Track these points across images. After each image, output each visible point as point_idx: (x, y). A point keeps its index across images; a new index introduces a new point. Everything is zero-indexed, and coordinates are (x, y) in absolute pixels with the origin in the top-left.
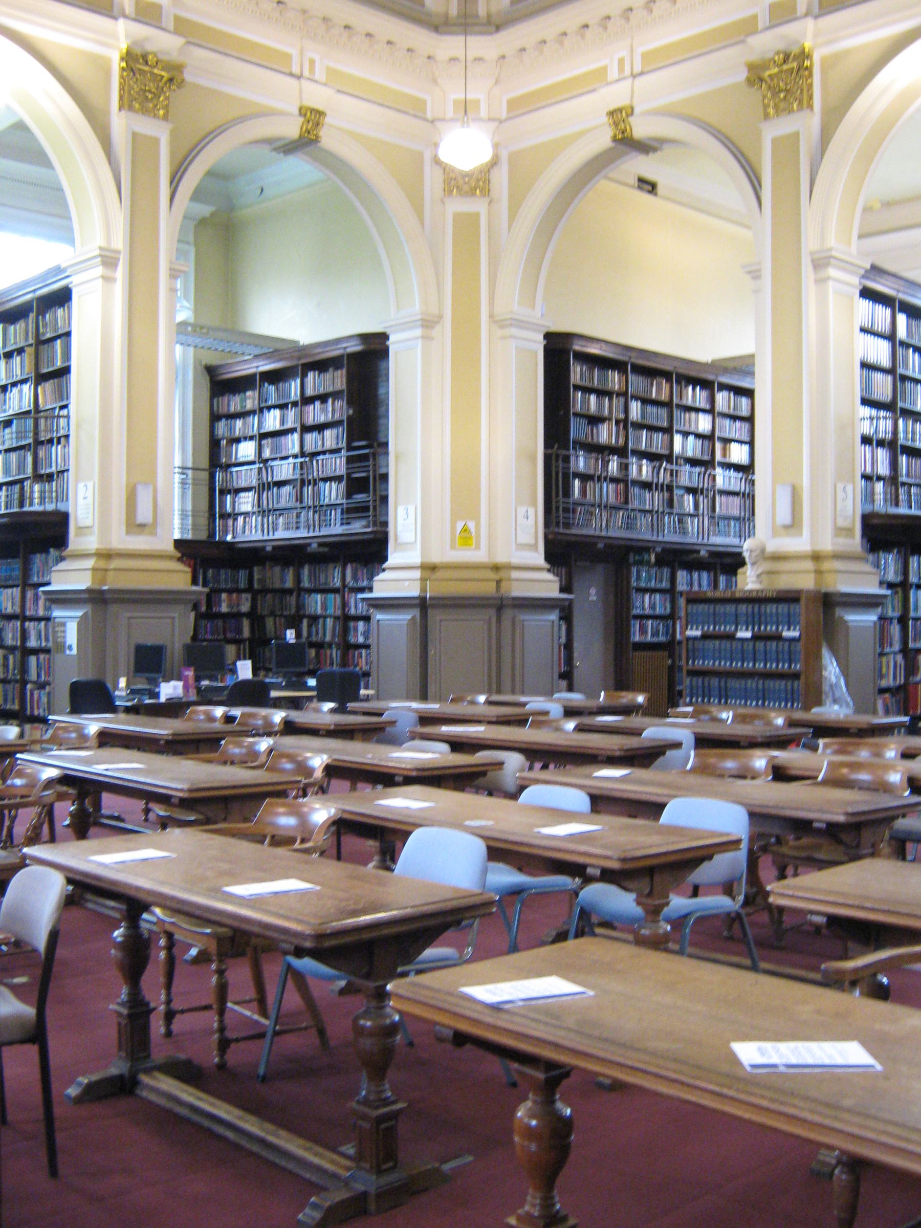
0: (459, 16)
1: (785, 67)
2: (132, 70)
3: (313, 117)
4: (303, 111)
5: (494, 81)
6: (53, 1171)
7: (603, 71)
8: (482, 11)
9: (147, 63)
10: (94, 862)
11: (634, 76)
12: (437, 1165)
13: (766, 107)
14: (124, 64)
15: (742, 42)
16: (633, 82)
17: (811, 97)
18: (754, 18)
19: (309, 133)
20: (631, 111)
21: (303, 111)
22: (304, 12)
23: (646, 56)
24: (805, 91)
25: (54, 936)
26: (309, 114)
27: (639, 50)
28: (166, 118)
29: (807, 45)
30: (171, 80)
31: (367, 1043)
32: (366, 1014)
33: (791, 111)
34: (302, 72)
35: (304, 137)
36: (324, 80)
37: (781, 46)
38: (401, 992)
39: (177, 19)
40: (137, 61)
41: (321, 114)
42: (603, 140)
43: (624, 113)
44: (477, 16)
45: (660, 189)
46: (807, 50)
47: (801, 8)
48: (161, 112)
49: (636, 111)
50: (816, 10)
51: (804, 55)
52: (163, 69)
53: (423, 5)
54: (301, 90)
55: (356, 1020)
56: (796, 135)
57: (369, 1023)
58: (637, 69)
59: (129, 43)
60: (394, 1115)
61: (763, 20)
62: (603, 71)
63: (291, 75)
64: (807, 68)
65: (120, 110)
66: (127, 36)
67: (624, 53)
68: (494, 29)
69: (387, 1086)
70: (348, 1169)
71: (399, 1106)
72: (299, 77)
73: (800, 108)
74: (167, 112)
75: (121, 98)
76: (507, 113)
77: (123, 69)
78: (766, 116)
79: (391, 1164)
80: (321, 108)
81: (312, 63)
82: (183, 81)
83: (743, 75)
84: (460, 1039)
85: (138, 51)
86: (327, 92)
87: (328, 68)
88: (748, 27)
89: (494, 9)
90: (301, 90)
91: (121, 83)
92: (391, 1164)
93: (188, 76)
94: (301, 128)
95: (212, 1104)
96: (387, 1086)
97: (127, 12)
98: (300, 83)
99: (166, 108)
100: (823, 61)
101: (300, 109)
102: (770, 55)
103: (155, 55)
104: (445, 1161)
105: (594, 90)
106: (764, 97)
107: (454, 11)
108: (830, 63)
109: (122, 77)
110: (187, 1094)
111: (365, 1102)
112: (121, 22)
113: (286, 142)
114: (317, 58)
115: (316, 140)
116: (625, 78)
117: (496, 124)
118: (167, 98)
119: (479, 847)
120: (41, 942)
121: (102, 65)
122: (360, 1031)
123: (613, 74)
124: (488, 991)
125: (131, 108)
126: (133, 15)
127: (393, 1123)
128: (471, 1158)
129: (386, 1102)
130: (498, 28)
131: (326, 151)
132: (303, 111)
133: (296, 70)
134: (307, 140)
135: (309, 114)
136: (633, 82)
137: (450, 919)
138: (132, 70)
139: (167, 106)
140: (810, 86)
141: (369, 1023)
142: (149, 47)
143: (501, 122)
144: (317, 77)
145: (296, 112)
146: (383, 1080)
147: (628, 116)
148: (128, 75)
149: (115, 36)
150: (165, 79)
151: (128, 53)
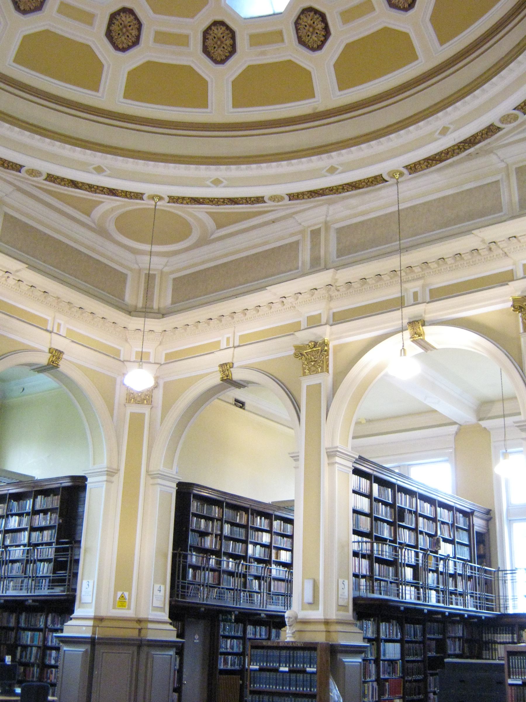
0: (142, 308)
1: (315, 349)
4: (51, 350)
5: (159, 343)
7: (219, 342)
8: (155, 306)
11: (235, 347)
13: (304, 369)
15: (293, 334)
16: (234, 350)
17: (328, 366)
18: (299, 323)
19: (53, 363)
20: (232, 365)
21: (51, 350)
22: (59, 298)
23: (241, 337)
24: (325, 362)
26: (54, 352)
27: (238, 334)
29: (327, 338)
33: (317, 372)
34: (53, 330)
36: (65, 335)
37: (313, 338)
41: (61, 352)
42: (216, 379)
43: (228, 366)
44: (152, 308)
45: (247, 406)
46: (326, 341)
47: (324, 320)
49: (235, 365)
50: (331, 322)
51: (325, 344)
53: (123, 300)
54: (51, 339)
56: (320, 384)
58: (236, 344)
61: (304, 325)
62: (219, 342)
63: (47, 331)
64: (326, 351)
67: (230, 335)
68: (161, 316)
72: (51, 332)
73: (322, 371)
76: (165, 360)
78: (304, 374)
80: (62, 350)
81: (59, 325)
83: (292, 352)
86: (67, 342)
87: (68, 329)
88: (295, 328)
89: (162, 306)
90: (51, 339)
94: (49, 360)
98: (51, 336)
100: (335, 347)
101: (50, 349)
102: (307, 343)
105: (213, 353)
106: (303, 364)
107: (140, 305)
108: (338, 349)
113: (39, 366)
114: (62, 323)
115: (57, 367)
116: (230, 348)
117: (158, 366)
123: (224, 345)
130: (163, 315)
132: (51, 351)
135: (54, 352)
136: (234, 350)
140: (327, 360)
143: (161, 365)
145: (47, 350)
147: (230, 368)
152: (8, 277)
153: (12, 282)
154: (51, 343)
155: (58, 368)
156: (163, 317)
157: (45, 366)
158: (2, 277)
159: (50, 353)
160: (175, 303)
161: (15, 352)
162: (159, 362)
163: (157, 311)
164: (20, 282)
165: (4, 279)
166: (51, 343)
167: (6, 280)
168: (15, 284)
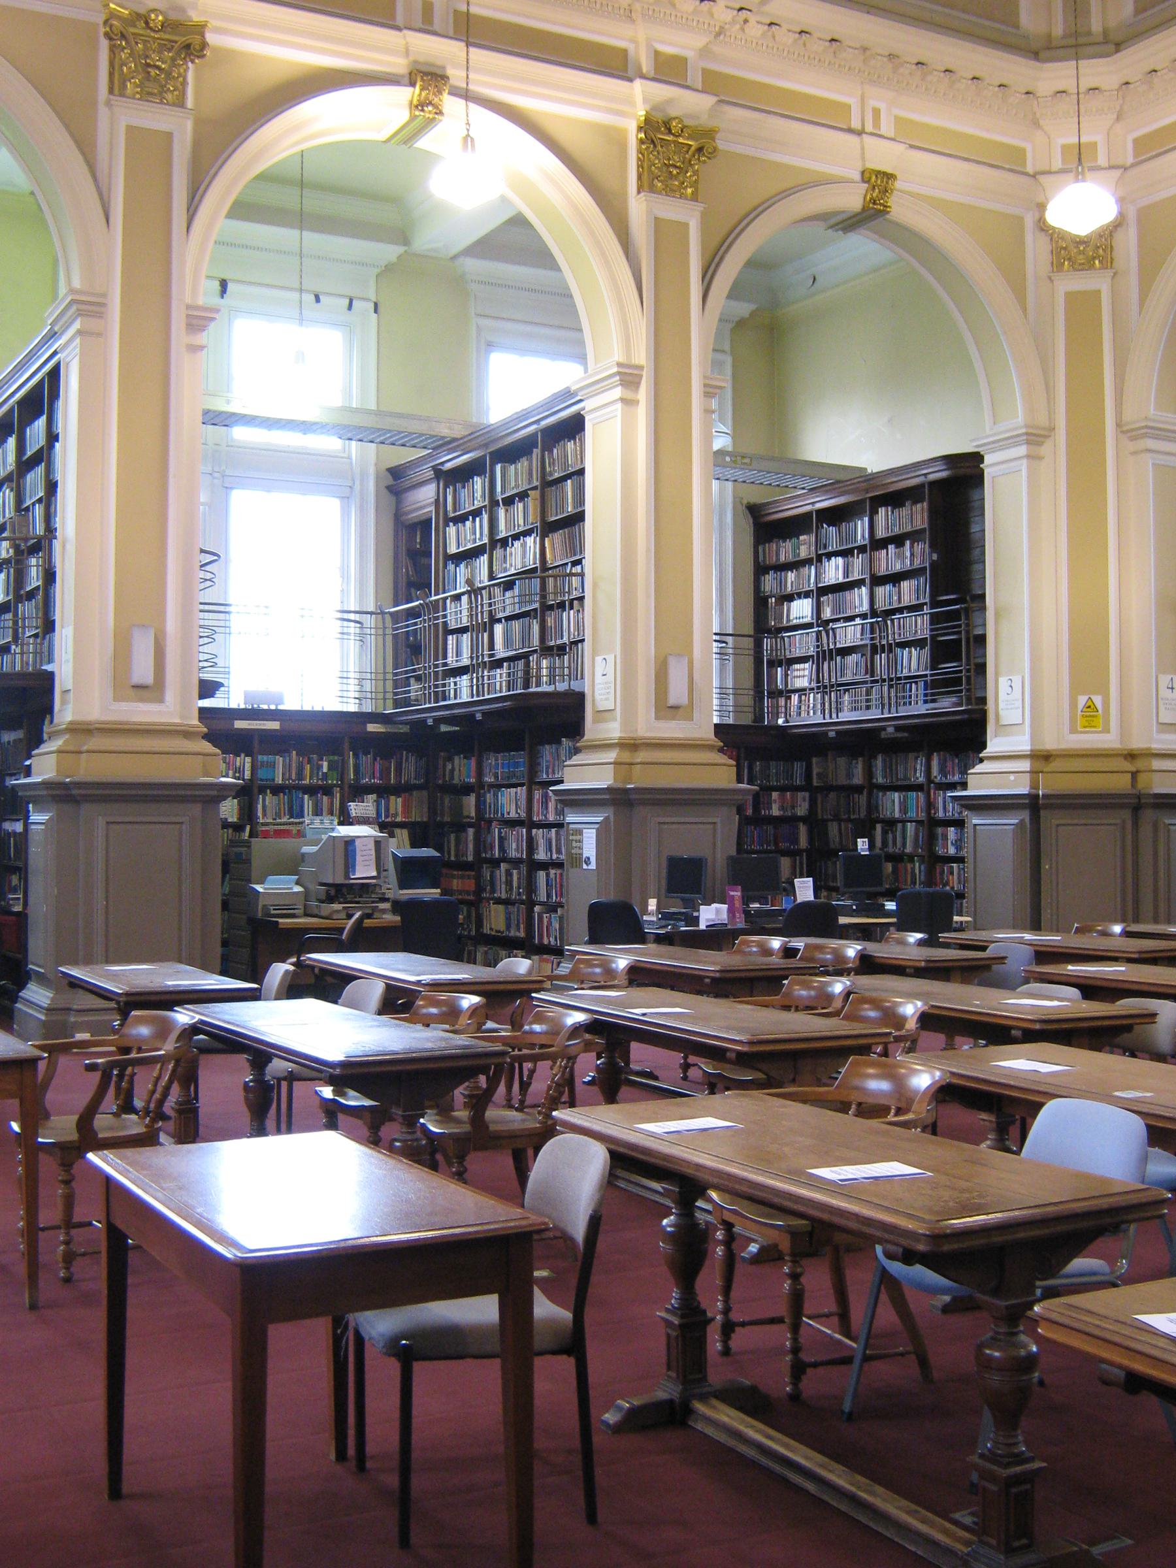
0: (1064, 37)
2: (653, 142)
3: (879, 182)
4: (867, 175)
5: (1115, 116)
6: (592, 1518)
8: (1096, 26)
9: (670, 131)
10: (642, 1132)
12: (1085, 1547)
14: (642, 135)
21: (867, 175)
22: (865, 49)
25: (595, 1223)
28: (695, 198)
30: (700, 150)
31: (995, 1380)
32: (994, 1342)
34: (863, 125)
35: (869, 209)
36: (892, 135)
38: (1054, 1316)
39: (705, 72)
40: (658, 130)
41: (890, 177)
44: (1089, 33)
48: (689, 191)
52: (688, 139)
53: (1017, 27)
54: (863, 149)
55: (981, 1347)
57: (997, 1354)
59: (648, 108)
60: (1029, 1478)
63: (850, 131)
65: (639, 192)
66: (645, 100)
68: (1112, 47)
69: (1020, 1438)
70: (968, 1543)
71: (1037, 1465)
72: (860, 133)
74: (697, 189)
75: (640, 177)
76: (1135, 156)
77: (642, 142)
79: (1024, 1541)
80: (889, 171)
81: (876, 113)
82: (715, 149)
84: (1135, 1383)
85: (659, 117)
86: (900, 148)
87: (896, 117)
89: (1112, 24)
90: (863, 149)
91: (639, 159)
92: (1024, 1541)
93: (720, 144)
95: (787, 1446)
96: (1020, 1438)
97: (644, 71)
98: (862, 142)
99: (695, 185)
101: (863, 173)
103: (681, 121)
104: (1093, 1543)
107: (1058, 30)
109: (640, 151)
110: (754, 1431)
111: (992, 1457)
112: (638, 84)
113: (844, 216)
114: (882, 106)
115: (884, 212)
117: (1118, 173)
118: (696, 173)
119: (1137, 1125)
120: (579, 1231)
121: (614, 137)
122: (986, 1364)
124: (1171, 1321)
125: (652, 189)
126: (652, 74)
127: (1028, 1486)
128: (1129, 1542)
129: (1020, 1459)
130: (1118, 46)
131: (896, 224)
133: (856, 124)
134: (872, 212)
137: (1108, 1220)
138: (653, 142)
139: (696, 181)
141: (997, 1354)
142: (673, 113)
143: (1126, 169)
144: (883, 132)
146: (1015, 1429)
148: (648, 148)
149: (631, 102)
150: (693, 149)
151: (647, 120)
152: (746, 21)
153: (755, 30)
154: (863, 159)
155: (888, 212)
156: (1117, 51)
157: (858, 214)
158: (733, 22)
159: (863, 181)
160: (1145, 10)
161: (785, 194)
162: (1120, 162)
163: (1101, 39)
164: (774, 27)
165: (738, 26)
166: (863, 159)
167: (743, 30)
168: (764, 35)
